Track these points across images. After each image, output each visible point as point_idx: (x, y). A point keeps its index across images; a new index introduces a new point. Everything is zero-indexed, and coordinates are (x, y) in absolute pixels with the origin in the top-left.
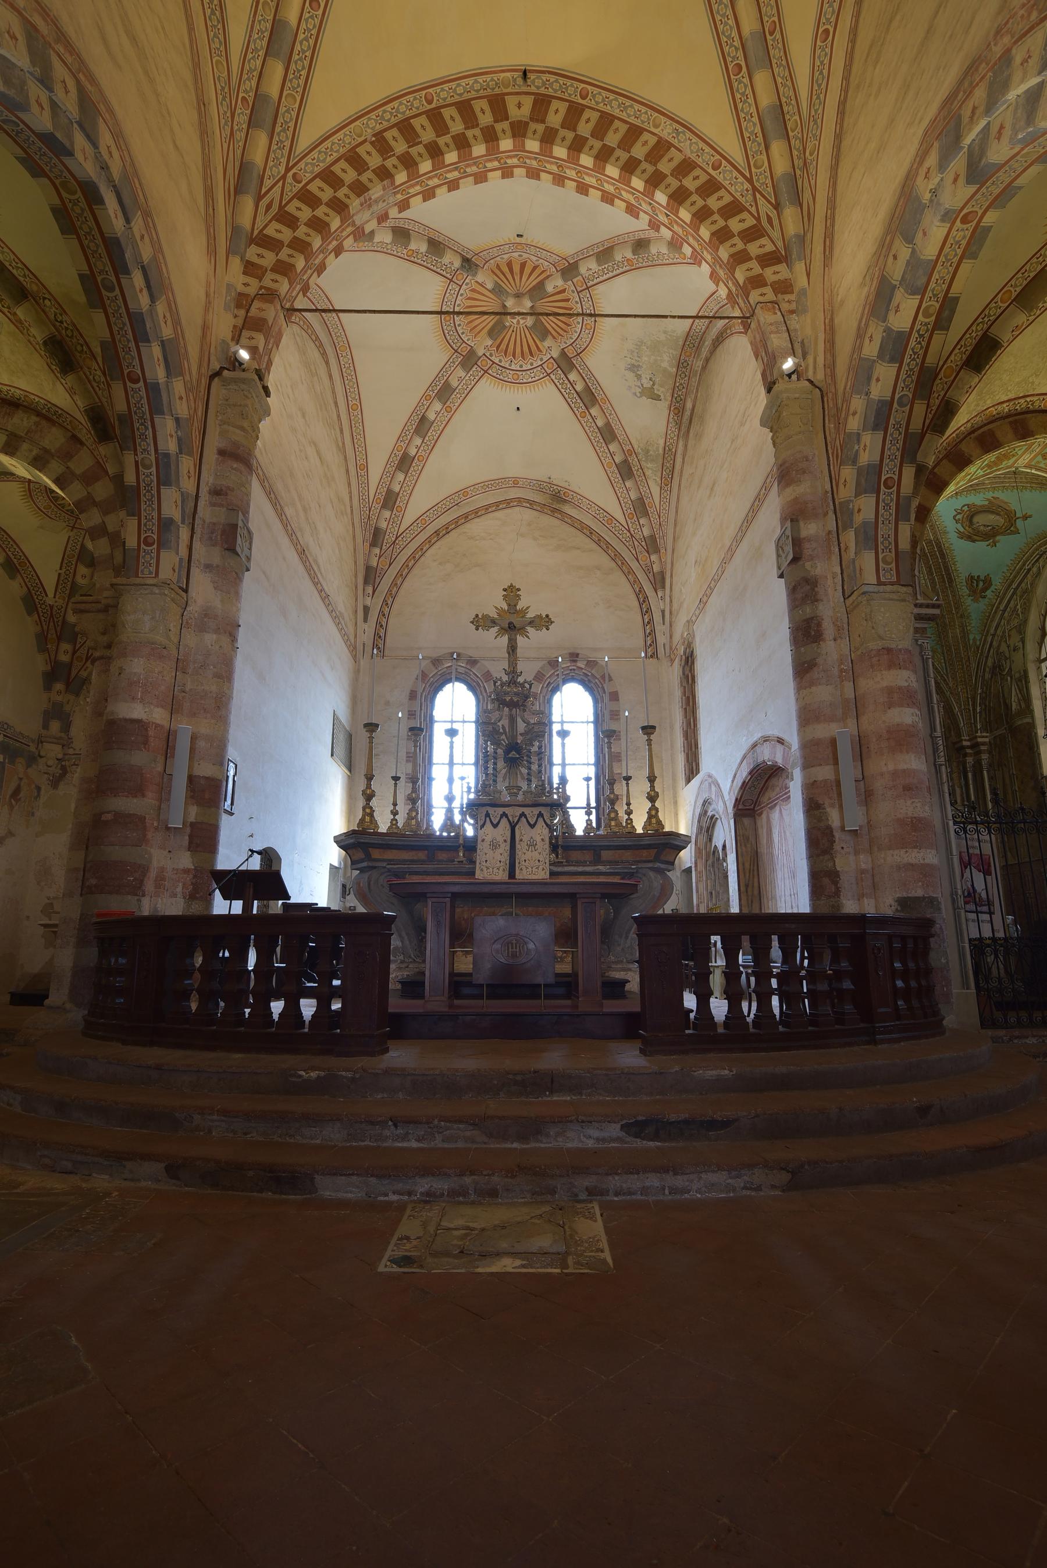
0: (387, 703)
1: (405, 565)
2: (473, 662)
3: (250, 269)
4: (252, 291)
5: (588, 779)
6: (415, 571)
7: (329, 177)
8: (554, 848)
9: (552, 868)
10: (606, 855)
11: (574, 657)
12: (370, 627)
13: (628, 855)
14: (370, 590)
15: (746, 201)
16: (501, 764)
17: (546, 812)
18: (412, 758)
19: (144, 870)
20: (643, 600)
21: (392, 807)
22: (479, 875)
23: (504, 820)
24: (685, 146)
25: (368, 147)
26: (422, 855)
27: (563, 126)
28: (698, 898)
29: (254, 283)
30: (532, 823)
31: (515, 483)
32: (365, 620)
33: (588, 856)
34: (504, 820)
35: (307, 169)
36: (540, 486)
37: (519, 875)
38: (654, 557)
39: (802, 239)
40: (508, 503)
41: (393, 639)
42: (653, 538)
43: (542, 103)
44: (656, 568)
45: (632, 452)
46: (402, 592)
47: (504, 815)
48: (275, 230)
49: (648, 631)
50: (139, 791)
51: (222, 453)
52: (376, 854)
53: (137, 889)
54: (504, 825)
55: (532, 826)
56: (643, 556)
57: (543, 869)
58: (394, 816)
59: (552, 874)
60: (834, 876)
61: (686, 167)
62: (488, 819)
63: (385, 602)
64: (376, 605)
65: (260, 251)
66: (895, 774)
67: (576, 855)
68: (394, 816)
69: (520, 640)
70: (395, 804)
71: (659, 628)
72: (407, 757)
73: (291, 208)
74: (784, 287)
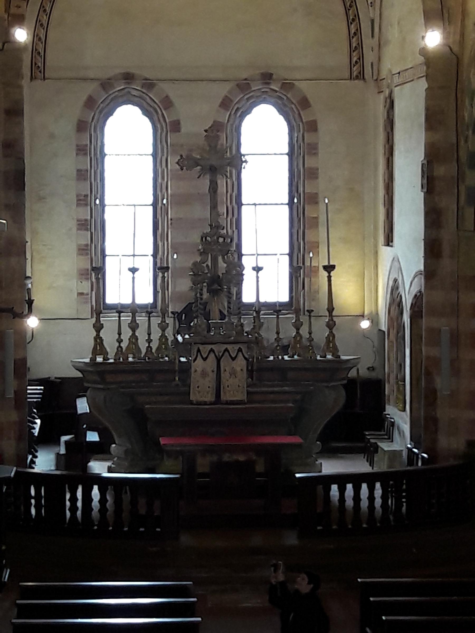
8: (250, 372)
9: (249, 389)
21: (117, 336)
22: (192, 397)
23: (212, 355)
28: (389, 367)
30: (233, 356)
34: (212, 355)
47: (212, 350)
49: (354, 45)
52: (109, 378)
54: (212, 358)
55: (233, 359)
57: (242, 392)
58: (120, 343)
59: (248, 393)
60: (435, 421)
62: (199, 354)
68: (120, 343)
70: (120, 334)
72: (78, 200)
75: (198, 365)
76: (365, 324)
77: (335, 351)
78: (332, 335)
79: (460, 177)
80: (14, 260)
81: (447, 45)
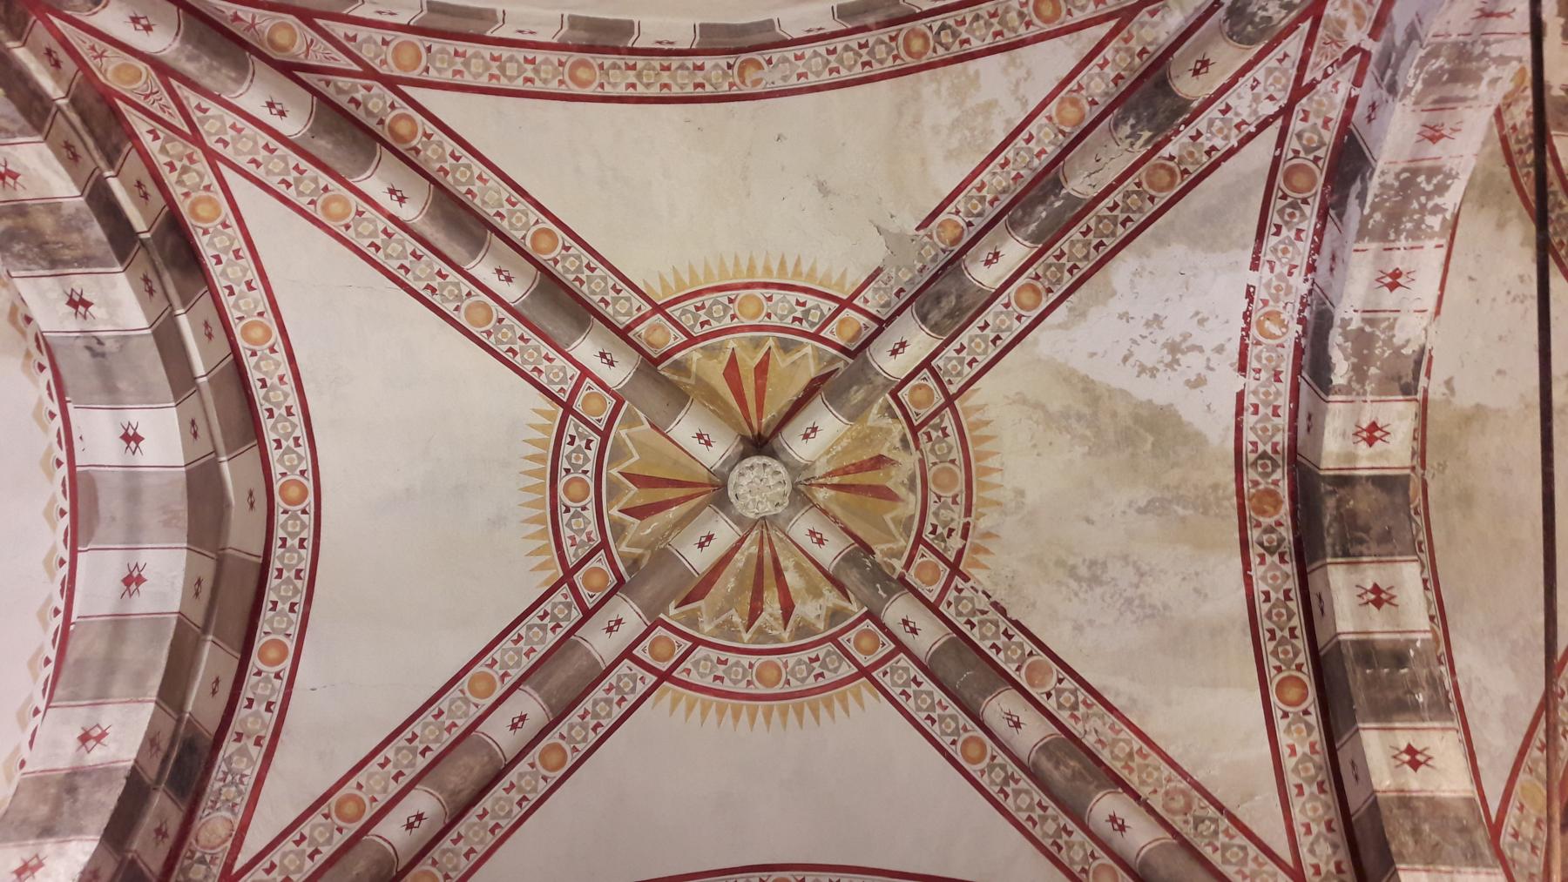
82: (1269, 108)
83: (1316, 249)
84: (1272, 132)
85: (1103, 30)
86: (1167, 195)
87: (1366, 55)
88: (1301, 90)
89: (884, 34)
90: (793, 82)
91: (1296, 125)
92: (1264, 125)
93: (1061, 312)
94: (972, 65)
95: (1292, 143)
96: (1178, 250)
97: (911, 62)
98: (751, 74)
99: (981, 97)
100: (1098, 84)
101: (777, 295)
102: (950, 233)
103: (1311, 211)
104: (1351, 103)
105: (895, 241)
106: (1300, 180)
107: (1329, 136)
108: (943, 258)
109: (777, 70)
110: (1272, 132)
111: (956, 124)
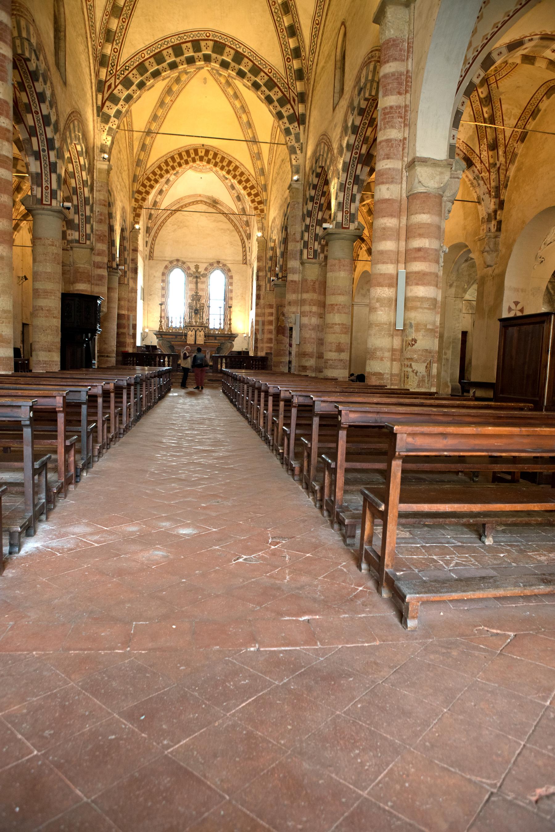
0: (154, 276)
1: (160, 225)
2: (184, 263)
3: (136, 200)
4: (136, 206)
5: (220, 308)
6: (163, 228)
7: (154, 173)
8: (205, 336)
10: (217, 338)
11: (218, 262)
12: (148, 249)
13: (223, 338)
14: (148, 235)
15: (256, 186)
16: (193, 314)
17: (203, 328)
18: (163, 296)
19: (126, 342)
20: (243, 243)
22: (188, 342)
24: (242, 169)
25: (163, 164)
26: (174, 337)
27: (213, 158)
29: (137, 204)
31: (200, 195)
32: (146, 246)
33: (213, 338)
35: (148, 172)
36: (209, 198)
37: (197, 343)
38: (248, 228)
39: (266, 200)
40: (197, 202)
41: (156, 254)
42: (247, 222)
43: (207, 152)
44: (248, 232)
45: (240, 194)
46: (159, 235)
48: (142, 189)
50: (125, 328)
51: (133, 250)
52: (163, 336)
53: (125, 347)
54: (194, 331)
56: (244, 226)
61: (242, 174)
63: (153, 239)
64: (150, 240)
65: (138, 195)
66: (268, 329)
67: (210, 338)
69: (199, 280)
71: (248, 253)
73: (145, 182)
74: (262, 211)
75: (190, 333)
76: (245, 335)
77: (231, 331)
78: (230, 327)
79: (266, 275)
80: (133, 294)
81: (263, 236)
82: (482, 156)
83: (461, 150)
84: (479, 155)
85: (506, 142)
86: (480, 135)
87: (480, 174)
88: (482, 162)
89: (533, 109)
90: (539, 91)
91: (478, 158)
92: (480, 154)
93: (472, 113)
94: (517, 120)
95: (476, 156)
96: (471, 133)
97: (526, 111)
98: (546, 87)
99: (512, 118)
100: (501, 137)
101: (506, 73)
102: (496, 102)
103: (466, 153)
104: (476, 167)
105: (501, 93)
106: (471, 154)
107: (474, 161)
108: (493, 99)
109: (543, 90)
110: (479, 155)
111: (511, 112)
